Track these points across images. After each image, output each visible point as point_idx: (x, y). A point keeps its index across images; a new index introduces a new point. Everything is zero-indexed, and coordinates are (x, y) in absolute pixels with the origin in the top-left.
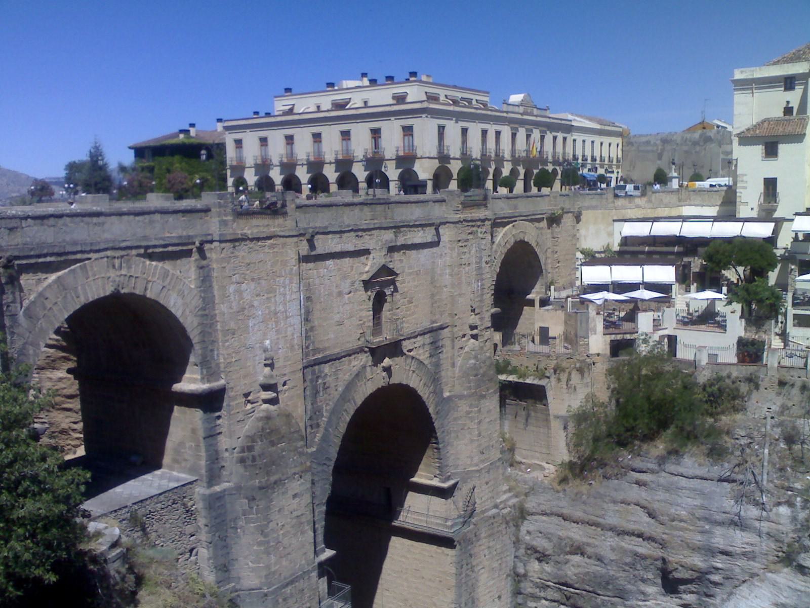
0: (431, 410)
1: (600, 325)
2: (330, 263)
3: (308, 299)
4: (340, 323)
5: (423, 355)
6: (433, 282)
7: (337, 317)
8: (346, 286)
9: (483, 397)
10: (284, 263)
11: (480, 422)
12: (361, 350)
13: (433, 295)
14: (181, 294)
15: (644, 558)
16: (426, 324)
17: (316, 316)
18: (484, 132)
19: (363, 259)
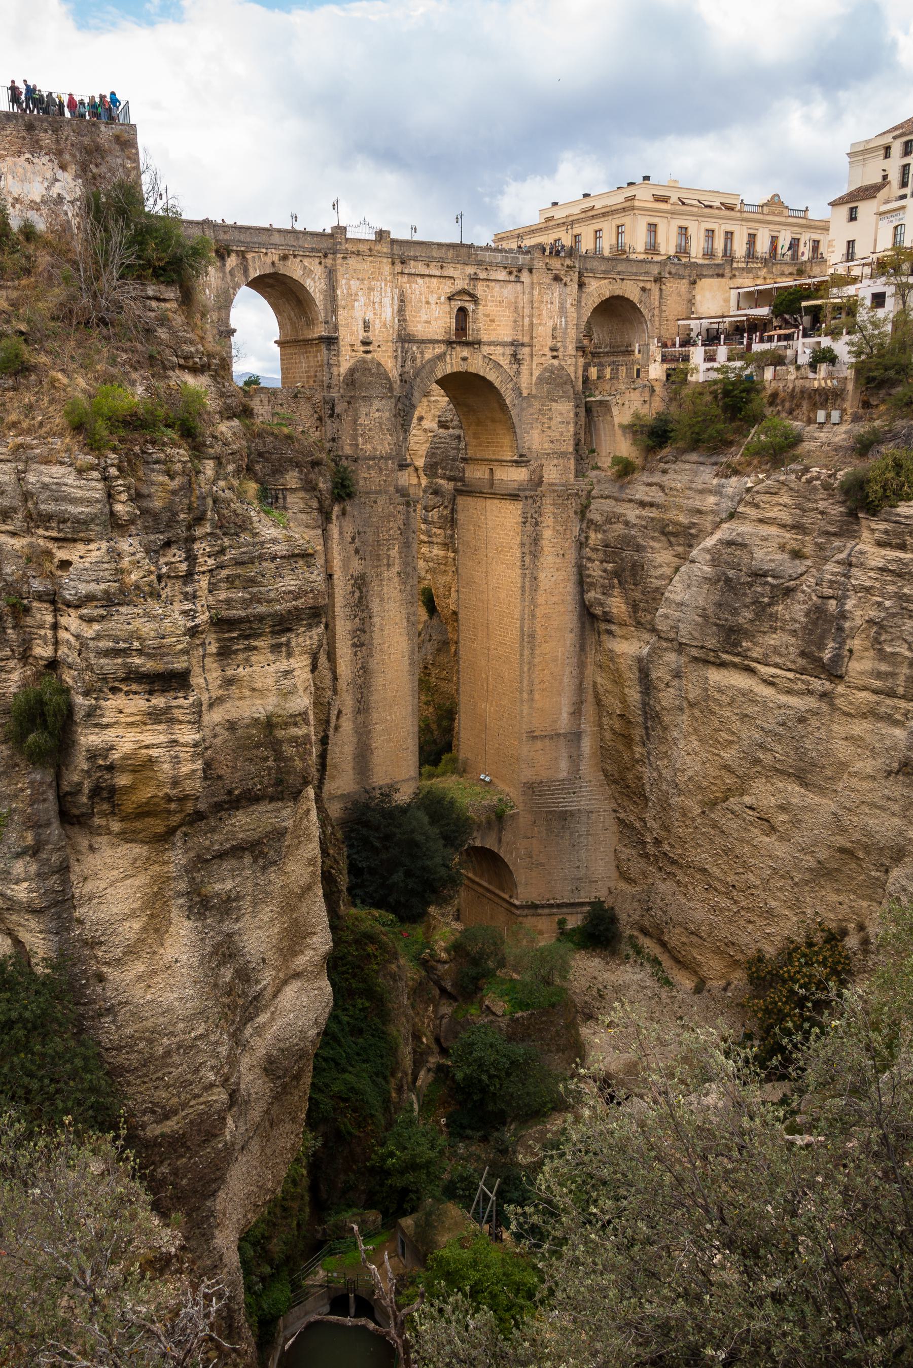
0: (508, 402)
1: (659, 358)
2: (420, 281)
3: (402, 301)
4: (428, 322)
5: (504, 362)
6: (516, 309)
7: (424, 318)
8: (433, 299)
9: (556, 401)
10: (381, 274)
11: (550, 419)
12: (442, 342)
13: (515, 321)
14: (313, 279)
15: (652, 519)
16: (508, 339)
17: (408, 314)
18: (710, 233)
19: (449, 282)
